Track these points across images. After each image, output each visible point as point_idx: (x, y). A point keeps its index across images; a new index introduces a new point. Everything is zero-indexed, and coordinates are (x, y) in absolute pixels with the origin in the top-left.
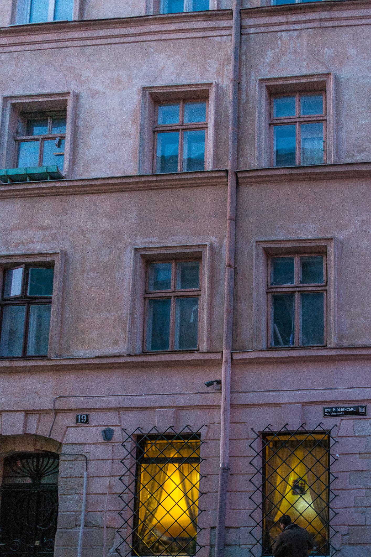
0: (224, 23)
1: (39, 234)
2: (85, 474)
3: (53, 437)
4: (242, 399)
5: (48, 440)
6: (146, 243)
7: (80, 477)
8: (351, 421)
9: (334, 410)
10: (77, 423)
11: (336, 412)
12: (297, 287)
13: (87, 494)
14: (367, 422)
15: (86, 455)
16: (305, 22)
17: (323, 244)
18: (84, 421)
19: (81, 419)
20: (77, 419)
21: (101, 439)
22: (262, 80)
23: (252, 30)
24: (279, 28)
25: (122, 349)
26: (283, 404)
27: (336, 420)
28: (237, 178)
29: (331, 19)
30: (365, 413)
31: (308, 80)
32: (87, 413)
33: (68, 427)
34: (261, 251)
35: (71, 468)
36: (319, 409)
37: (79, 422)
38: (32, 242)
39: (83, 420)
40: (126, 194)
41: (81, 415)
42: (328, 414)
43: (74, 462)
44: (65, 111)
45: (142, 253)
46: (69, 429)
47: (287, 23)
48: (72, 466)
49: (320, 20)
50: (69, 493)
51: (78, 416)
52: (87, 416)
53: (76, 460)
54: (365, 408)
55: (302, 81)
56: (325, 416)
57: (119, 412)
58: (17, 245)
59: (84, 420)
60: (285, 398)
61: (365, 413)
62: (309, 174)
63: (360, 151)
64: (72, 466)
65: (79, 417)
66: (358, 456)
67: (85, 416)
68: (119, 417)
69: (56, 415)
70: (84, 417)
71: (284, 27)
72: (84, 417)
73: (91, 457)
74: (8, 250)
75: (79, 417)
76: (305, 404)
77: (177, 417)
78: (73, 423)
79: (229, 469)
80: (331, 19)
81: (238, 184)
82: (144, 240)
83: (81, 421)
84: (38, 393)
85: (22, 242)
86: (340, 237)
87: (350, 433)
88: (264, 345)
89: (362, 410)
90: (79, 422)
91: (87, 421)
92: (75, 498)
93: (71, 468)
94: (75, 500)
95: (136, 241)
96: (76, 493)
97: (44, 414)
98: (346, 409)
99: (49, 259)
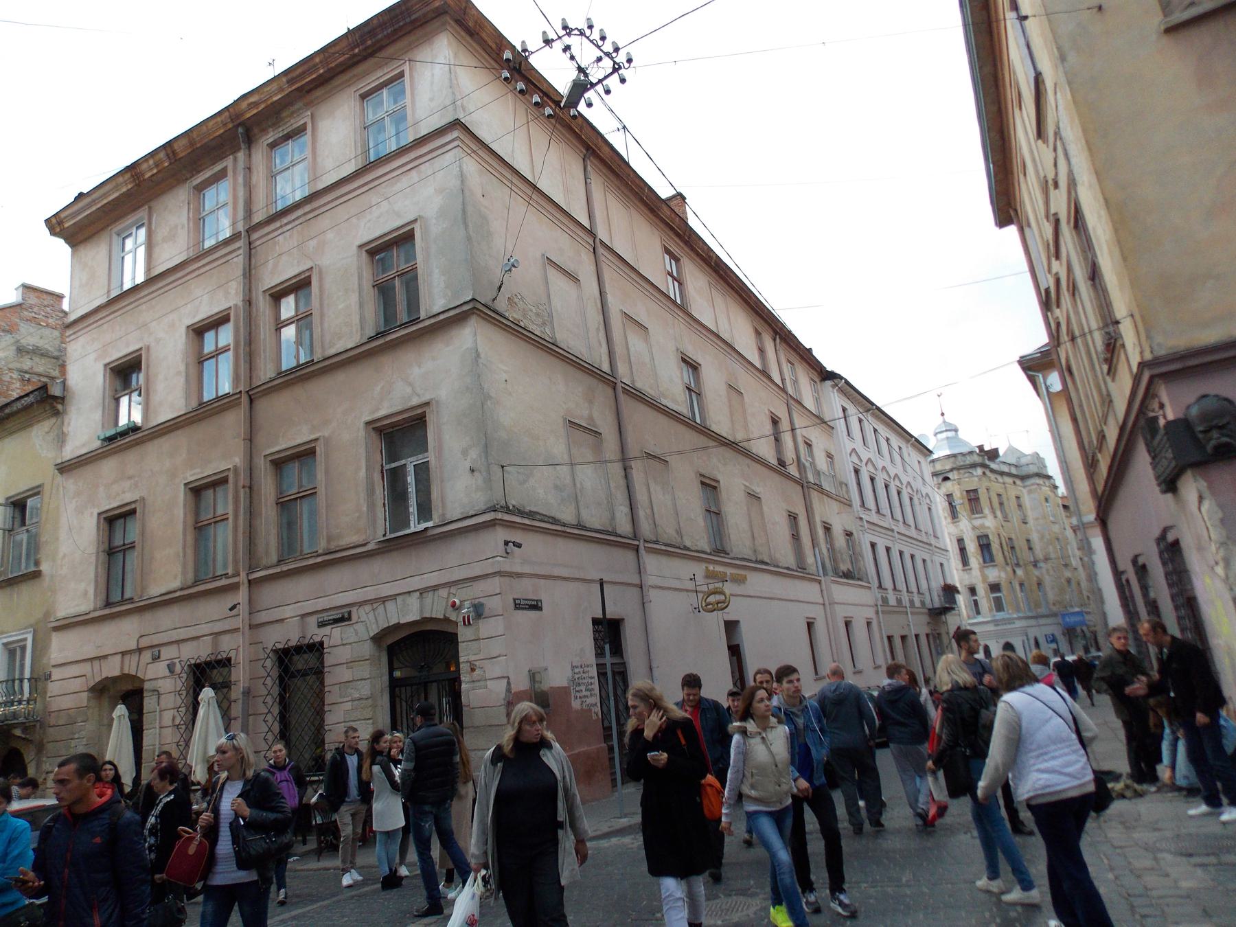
0: (237, 245)
1: (127, 484)
4: (263, 617)
5: (134, 677)
6: (194, 474)
12: (298, 493)
13: (161, 728)
14: (352, 630)
16: (294, 220)
21: (167, 673)
22: (264, 291)
23: (258, 243)
24: (276, 234)
25: (176, 584)
26: (287, 619)
27: (327, 630)
28: (250, 396)
29: (313, 210)
30: (349, 619)
31: (298, 279)
34: (268, 464)
36: (313, 620)
42: (322, 625)
44: (140, 362)
45: (190, 486)
47: (281, 227)
49: (305, 214)
52: (159, 651)
54: (350, 613)
55: (294, 281)
56: (319, 626)
60: (288, 612)
62: (300, 376)
66: (345, 665)
69: (140, 654)
71: (280, 231)
73: (161, 691)
76: (303, 616)
77: (215, 644)
80: (313, 210)
81: (251, 401)
82: (192, 472)
84: (128, 634)
86: (326, 433)
87: (339, 642)
88: (274, 558)
89: (346, 615)
98: (334, 617)
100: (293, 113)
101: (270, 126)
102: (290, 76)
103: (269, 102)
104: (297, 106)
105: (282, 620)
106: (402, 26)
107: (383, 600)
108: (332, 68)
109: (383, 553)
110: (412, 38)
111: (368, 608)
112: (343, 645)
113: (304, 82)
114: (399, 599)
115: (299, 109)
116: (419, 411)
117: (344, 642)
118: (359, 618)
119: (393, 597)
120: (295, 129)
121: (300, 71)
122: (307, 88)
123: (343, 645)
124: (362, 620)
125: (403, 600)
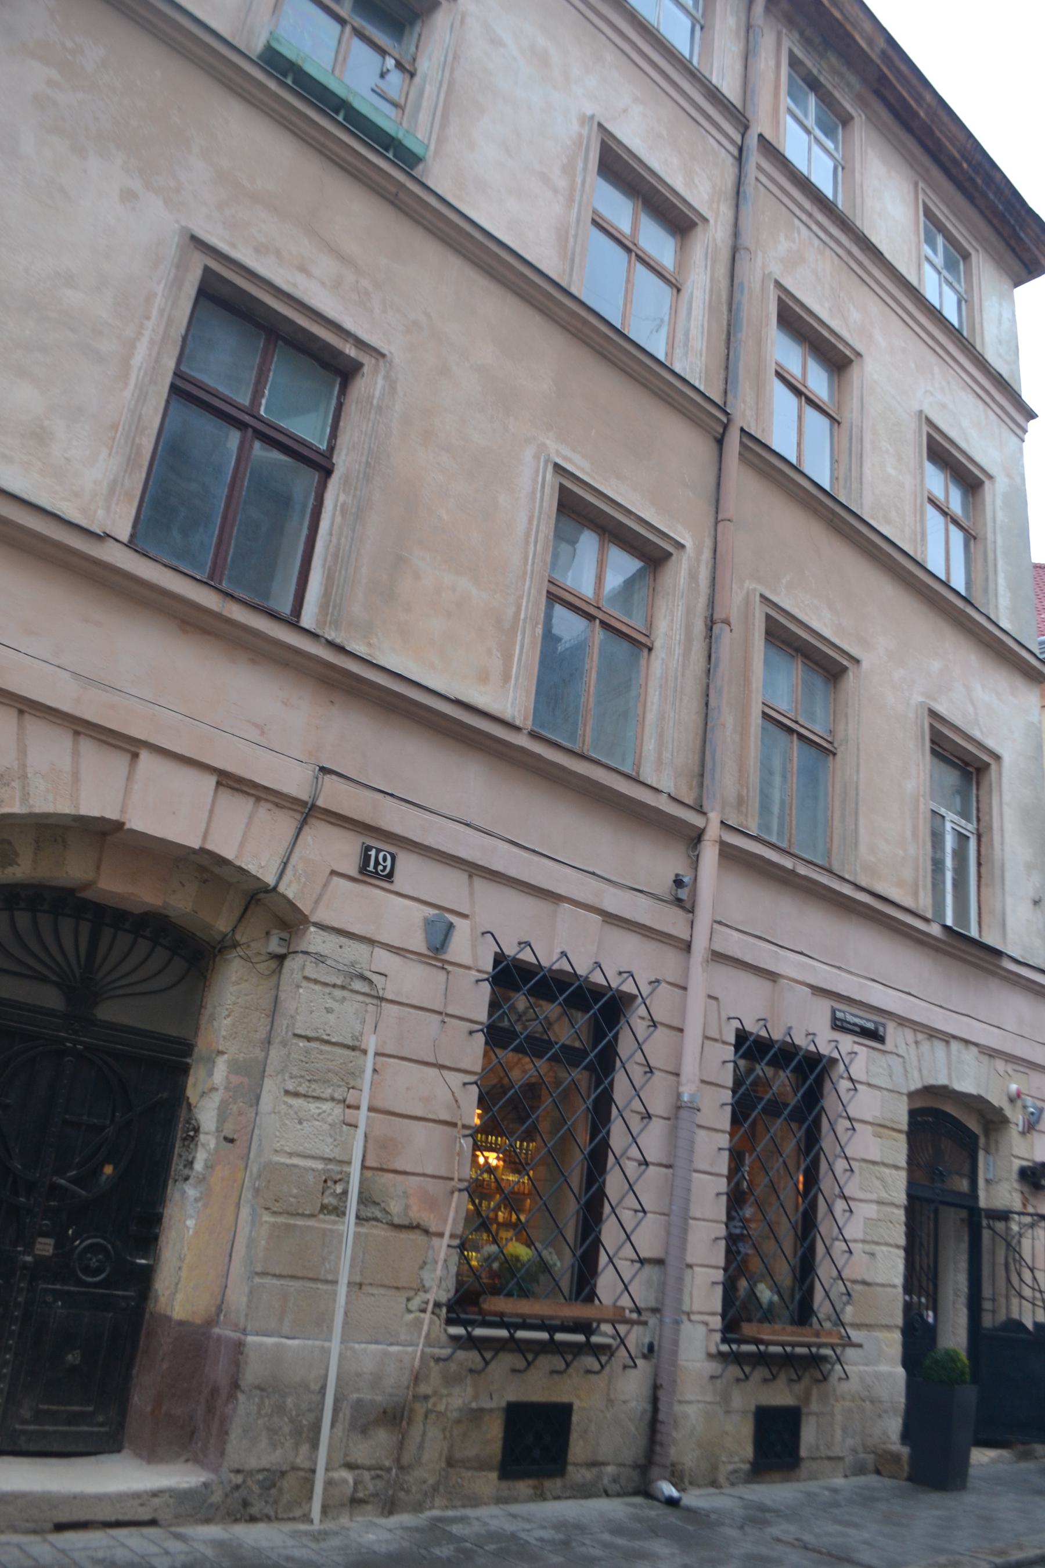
1: (325, 266)
2: (371, 1044)
3: (289, 889)
7: (353, 1048)
8: (864, 1048)
9: (849, 1018)
10: (363, 869)
11: (849, 1023)
15: (375, 978)
17: (845, 663)
18: (382, 871)
19: (377, 863)
20: (366, 859)
21: (418, 942)
24: (798, 212)
27: (847, 1042)
31: (833, 340)
32: (393, 850)
33: (334, 873)
35: (329, 1011)
37: (371, 868)
38: (303, 269)
39: (380, 868)
40: (538, 318)
41: (378, 851)
42: (839, 1025)
43: (338, 993)
46: (336, 880)
47: (810, 215)
48: (330, 1003)
50: (315, 1094)
51: (368, 848)
53: (343, 987)
54: (884, 1026)
55: (826, 334)
57: (470, 876)
58: (260, 250)
59: (385, 867)
60: (787, 965)
61: (881, 1039)
63: (888, 521)
64: (330, 1003)
65: (373, 853)
67: (389, 857)
68: (472, 894)
69: (304, 823)
70: (385, 860)
72: (385, 860)
74: (233, 246)
75: (373, 853)
78: (351, 867)
79: (699, 1110)
80: (860, 264)
83: (376, 867)
85: (278, 253)
89: (881, 1029)
90: (371, 868)
91: (390, 877)
92: (330, 1114)
93: (329, 1011)
94: (330, 1120)
95: (548, 442)
96: (333, 1099)
97: (269, 806)
99: (350, 351)
100: (841, 75)
101: (802, 34)
102: (891, 52)
103: (849, 28)
104: (853, 79)
105: (772, 976)
106: (1009, 222)
107: (933, 1034)
108: (931, 133)
109: (937, 950)
110: (993, 237)
111: (909, 1035)
112: (869, 1085)
113: (895, 82)
114: (955, 1045)
115: (848, 84)
116: (985, 758)
117: (873, 1081)
118: (896, 1046)
119: (947, 1038)
120: (831, 95)
121: (903, 67)
122: (887, 93)
123: (869, 1085)
124: (901, 1052)
125: (959, 1052)
